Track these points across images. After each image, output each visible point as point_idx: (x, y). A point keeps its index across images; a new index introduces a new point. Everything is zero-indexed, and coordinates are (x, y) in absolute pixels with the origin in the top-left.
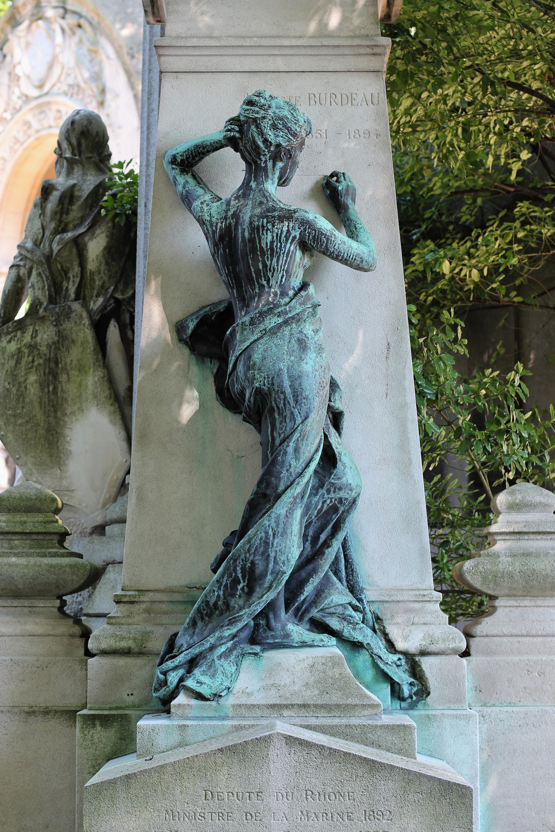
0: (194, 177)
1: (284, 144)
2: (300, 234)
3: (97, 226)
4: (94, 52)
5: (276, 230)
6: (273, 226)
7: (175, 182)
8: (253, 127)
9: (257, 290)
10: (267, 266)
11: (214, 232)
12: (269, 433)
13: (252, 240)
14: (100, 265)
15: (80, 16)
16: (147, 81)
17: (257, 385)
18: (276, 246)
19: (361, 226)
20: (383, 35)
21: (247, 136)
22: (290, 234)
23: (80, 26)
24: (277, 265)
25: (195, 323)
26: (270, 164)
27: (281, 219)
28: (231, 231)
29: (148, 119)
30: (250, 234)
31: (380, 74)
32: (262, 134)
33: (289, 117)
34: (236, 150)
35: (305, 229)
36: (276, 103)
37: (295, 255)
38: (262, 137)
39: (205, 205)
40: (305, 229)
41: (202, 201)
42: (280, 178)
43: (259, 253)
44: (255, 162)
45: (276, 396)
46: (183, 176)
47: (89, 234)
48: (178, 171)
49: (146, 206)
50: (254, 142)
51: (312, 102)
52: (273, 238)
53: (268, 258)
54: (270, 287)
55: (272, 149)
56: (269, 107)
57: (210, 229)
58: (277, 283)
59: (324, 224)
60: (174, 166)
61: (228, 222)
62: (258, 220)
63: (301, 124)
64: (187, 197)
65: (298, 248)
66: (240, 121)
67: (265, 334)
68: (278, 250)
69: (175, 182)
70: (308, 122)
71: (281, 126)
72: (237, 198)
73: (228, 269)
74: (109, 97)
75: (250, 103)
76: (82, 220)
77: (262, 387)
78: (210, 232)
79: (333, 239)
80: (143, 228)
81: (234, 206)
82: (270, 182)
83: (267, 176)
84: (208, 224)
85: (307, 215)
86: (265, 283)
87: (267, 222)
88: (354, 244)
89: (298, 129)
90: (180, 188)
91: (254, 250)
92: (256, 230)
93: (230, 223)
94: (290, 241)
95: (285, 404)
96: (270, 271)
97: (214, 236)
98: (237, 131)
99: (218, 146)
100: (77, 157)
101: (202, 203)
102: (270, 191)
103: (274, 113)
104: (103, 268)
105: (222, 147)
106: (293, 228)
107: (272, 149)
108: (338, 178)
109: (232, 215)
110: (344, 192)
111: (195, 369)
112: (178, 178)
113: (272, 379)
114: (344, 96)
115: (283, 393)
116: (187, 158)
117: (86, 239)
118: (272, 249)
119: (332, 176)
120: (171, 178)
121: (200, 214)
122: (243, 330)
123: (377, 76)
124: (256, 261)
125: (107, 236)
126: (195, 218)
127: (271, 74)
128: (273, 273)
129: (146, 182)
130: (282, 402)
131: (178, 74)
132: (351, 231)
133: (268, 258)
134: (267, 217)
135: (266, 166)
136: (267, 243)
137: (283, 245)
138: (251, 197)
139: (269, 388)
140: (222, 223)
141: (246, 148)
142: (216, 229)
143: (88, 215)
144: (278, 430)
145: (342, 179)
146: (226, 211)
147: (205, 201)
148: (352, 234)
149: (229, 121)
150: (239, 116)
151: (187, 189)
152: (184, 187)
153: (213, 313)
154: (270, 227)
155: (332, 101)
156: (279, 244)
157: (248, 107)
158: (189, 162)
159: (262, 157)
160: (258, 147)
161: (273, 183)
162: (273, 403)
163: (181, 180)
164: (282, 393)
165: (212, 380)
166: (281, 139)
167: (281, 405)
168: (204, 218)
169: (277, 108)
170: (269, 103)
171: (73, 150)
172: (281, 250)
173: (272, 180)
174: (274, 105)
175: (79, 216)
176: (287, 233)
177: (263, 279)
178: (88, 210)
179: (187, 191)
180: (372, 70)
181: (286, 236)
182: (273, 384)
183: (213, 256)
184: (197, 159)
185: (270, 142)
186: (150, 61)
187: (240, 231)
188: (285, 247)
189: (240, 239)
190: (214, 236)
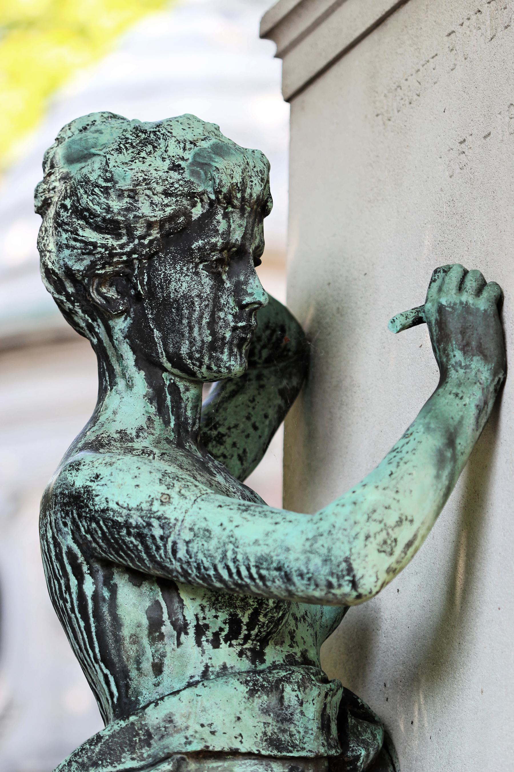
2: (75, 541)
79: (157, 532)
82: (121, 384)
137: (62, 582)
161: (130, 386)
169: (70, 160)
172: (65, 601)
173: (124, 376)
176: (55, 547)
188: (68, 587)
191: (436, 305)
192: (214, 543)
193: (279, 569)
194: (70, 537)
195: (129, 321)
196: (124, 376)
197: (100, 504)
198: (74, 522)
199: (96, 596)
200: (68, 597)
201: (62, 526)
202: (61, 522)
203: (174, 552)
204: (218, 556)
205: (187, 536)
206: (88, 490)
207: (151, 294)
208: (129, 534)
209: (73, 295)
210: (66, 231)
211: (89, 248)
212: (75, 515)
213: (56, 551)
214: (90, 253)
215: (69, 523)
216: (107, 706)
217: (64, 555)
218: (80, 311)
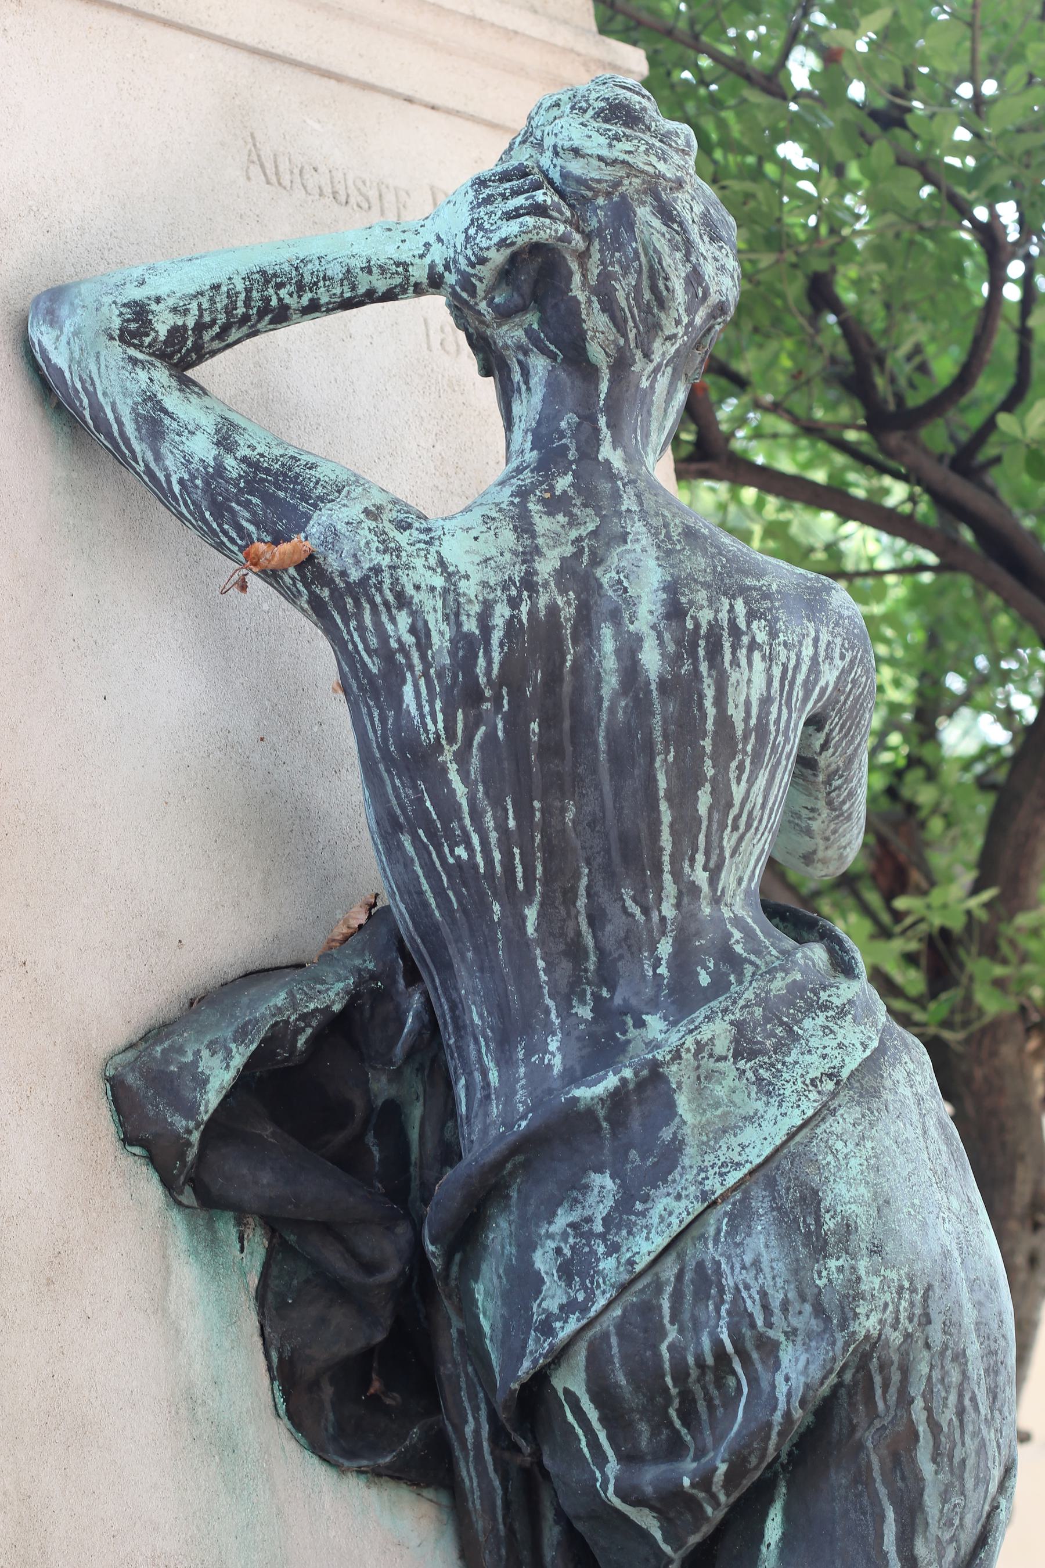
5: (783, 652)
6: (773, 634)
9: (668, 910)
10: (730, 805)
12: (890, 1543)
13: (681, 688)
17: (868, 1324)
18: (777, 722)
24: (763, 806)
25: (238, 1061)
26: (663, 382)
28: (560, 641)
30: (675, 660)
43: (707, 744)
45: (936, 1375)
53: (741, 768)
54: (717, 901)
58: (740, 881)
61: (543, 601)
67: (834, 1095)
68: (781, 739)
72: (554, 505)
73: (524, 813)
77: (888, 1330)
86: (701, 877)
87: (751, 616)
91: (686, 728)
93: (553, 610)
95: (961, 1412)
96: (735, 828)
109: (560, 574)
111: (187, 1275)
113: (926, 1297)
115: (960, 1357)
116: (200, 327)
122: (703, 1078)
124: (687, 781)
128: (741, 839)
130: (953, 1399)
133: (741, 768)
137: (794, 715)
139: (908, 1336)
140: (514, 603)
142: (486, 629)
144: (934, 1529)
146: (529, 555)
153: (303, 1017)
154: (761, 637)
162: (919, 1404)
164: (955, 1358)
165: (251, 1322)
167: (947, 1416)
176: (810, 671)
177: (700, 858)
181: (806, 682)
182: (927, 1319)
187: (608, 646)
189: (611, 683)
194: (836, 673)
198: (852, 662)
201: (837, 655)
202: (838, 650)
213: (808, 676)
215: (848, 659)
216: (733, 885)
218: (677, 345)
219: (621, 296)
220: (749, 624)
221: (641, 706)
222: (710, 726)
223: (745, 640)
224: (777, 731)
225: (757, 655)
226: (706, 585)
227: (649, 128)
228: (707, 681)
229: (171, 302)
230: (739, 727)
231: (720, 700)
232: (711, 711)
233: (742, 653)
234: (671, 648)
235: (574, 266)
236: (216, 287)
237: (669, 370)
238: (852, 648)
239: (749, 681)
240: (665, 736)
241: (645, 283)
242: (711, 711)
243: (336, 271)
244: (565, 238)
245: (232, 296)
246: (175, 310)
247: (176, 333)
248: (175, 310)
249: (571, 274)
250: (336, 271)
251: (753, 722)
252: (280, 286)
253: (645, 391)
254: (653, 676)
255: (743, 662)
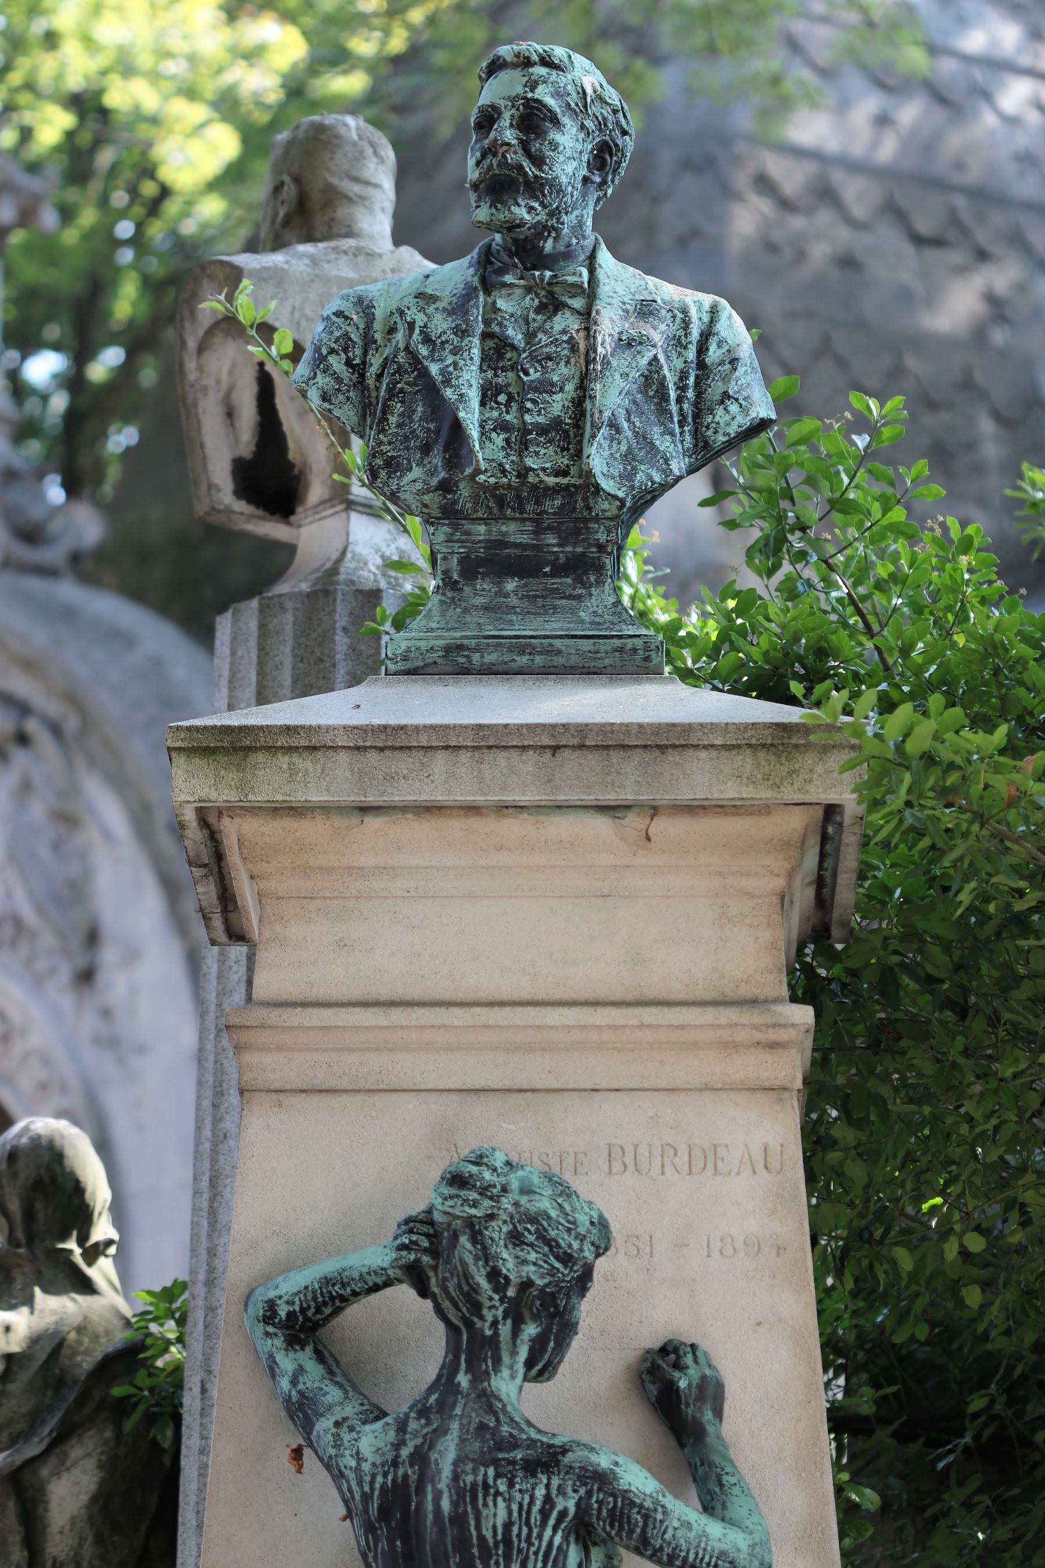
0: (320, 1357)
1: (540, 1282)
2: (578, 1505)
3: (74, 1441)
4: (67, 819)
5: (518, 1496)
6: (511, 1485)
7: (272, 1370)
8: (464, 1240)
11: (366, 1497)
13: (458, 1519)
14: (80, 1545)
15: (23, 709)
16: (212, 1058)
18: (519, 1536)
19: (733, 1480)
20: (794, 999)
21: (448, 1261)
22: (553, 1505)
23: (23, 739)
26: (505, 1330)
27: (531, 1468)
28: (409, 1494)
29: (214, 1161)
30: (455, 1504)
31: (786, 1095)
32: (486, 1256)
33: (553, 1213)
34: (424, 1291)
35: (589, 1494)
36: (522, 1180)
37: (566, 1557)
38: (486, 1263)
39: (345, 1429)
40: (589, 1494)
41: (339, 1418)
42: (529, 1364)
43: (475, 1551)
44: (469, 1324)
46: (291, 1355)
47: (53, 1461)
48: (279, 1342)
49: (204, 1390)
50: (467, 1276)
51: (617, 1166)
52: (510, 1513)
55: (511, 1292)
56: (505, 1189)
57: (356, 1488)
59: (638, 1480)
60: (271, 1329)
61: (400, 1472)
62: (475, 1471)
63: (582, 1230)
64: (301, 1407)
65: (572, 1539)
66: (431, 1223)
68: (524, 1545)
69: (272, 1370)
70: (602, 1225)
71: (531, 1238)
72: (423, 1412)
74: (108, 956)
75: (457, 1180)
76: (35, 1419)
78: (357, 1497)
79: (659, 1516)
80: (195, 1449)
81: (415, 1434)
82: (505, 1373)
83: (497, 1361)
84: (352, 1476)
85: (593, 1458)
87: (498, 1476)
88: (714, 1529)
89: (576, 1245)
90: (285, 1383)
91: (462, 1543)
92: (468, 1496)
93: (406, 1477)
94: (552, 1522)
97: (366, 1509)
98: (425, 1250)
99: (379, 1281)
100: (21, 1251)
101: (337, 1424)
102: (504, 1398)
103: (517, 1204)
104: (87, 1551)
105: (388, 1283)
106: (561, 1490)
107: (511, 1292)
108: (679, 1357)
109: (411, 1456)
110: (694, 1391)
112: (279, 1357)
114: (697, 1153)
116: (303, 1310)
117: (44, 1472)
118: (507, 1541)
119: (664, 1351)
120: (264, 1357)
121: (333, 1452)
123: (780, 1100)
125: (101, 1466)
126: (321, 1459)
127: (514, 1095)
129: (206, 1327)
131: (282, 1097)
132: (709, 1492)
134: (495, 1462)
135: (496, 1334)
136: (495, 1528)
137: (535, 1531)
138: (458, 1411)
140: (385, 1475)
141: (445, 1289)
142: (372, 1489)
143: (51, 1409)
145: (689, 1360)
146: (398, 1446)
147: (345, 1419)
148: (712, 1504)
149: (407, 1222)
150: (429, 1211)
151: (301, 1386)
152: (294, 1382)
154: (503, 1487)
155: (667, 1161)
156: (525, 1530)
157: (453, 1191)
158: (307, 1319)
159: (485, 1312)
160: (475, 1289)
161: (513, 1377)
163: (286, 1363)
166: (532, 1268)
168: (342, 1462)
170: (503, 1180)
171: (12, 1230)
172: (530, 1544)
173: (511, 1367)
174: (515, 1185)
175: (25, 1409)
178: (49, 1393)
179: (301, 1393)
180: (767, 1085)
181: (542, 1511)
183: (364, 1556)
184: (328, 1311)
185: (506, 1278)
186: (219, 1005)
188: (540, 1536)
189: (430, 1517)
190: (366, 1509)
191: (699, 1374)
192: (694, 1533)
193: (731, 1563)
195: (539, 1329)
196: (511, 1367)
197: (623, 1485)
199: (559, 1548)
200: (536, 1543)
201: (569, 1490)
203: (664, 1532)
204: (695, 1543)
205: (676, 1524)
206: (612, 1471)
207: (562, 1315)
208: (639, 1513)
209: (510, 1298)
210: (537, 1252)
211: (552, 1272)
212: (595, 1487)
214: (553, 1276)
217: (555, 1514)
219: (451, 1290)
220: (495, 1481)
221: (442, 1532)
222: (475, 1541)
223: (492, 1491)
224: (520, 1541)
225: (500, 1500)
226: (473, 1461)
227: (474, 1186)
228: (471, 1516)
229: (286, 1298)
230: (491, 1541)
231: (478, 1527)
232: (474, 1533)
233: (490, 1500)
234: (455, 1498)
235: (431, 1274)
236: (306, 1288)
237: (509, 1322)
238: (585, 1484)
239: (495, 1515)
240: (453, 1547)
241: (463, 1281)
242: (474, 1533)
243: (356, 1275)
244: (417, 1261)
245: (314, 1292)
246: (288, 1303)
247: (291, 1315)
248: (288, 1303)
249: (429, 1278)
250: (356, 1275)
251: (499, 1537)
252: (334, 1285)
253: (491, 1337)
254: (446, 1514)
255: (491, 1504)
